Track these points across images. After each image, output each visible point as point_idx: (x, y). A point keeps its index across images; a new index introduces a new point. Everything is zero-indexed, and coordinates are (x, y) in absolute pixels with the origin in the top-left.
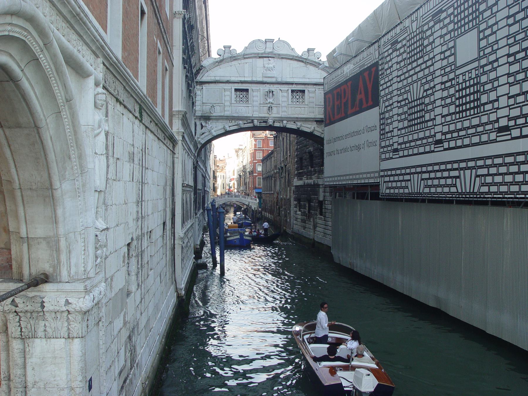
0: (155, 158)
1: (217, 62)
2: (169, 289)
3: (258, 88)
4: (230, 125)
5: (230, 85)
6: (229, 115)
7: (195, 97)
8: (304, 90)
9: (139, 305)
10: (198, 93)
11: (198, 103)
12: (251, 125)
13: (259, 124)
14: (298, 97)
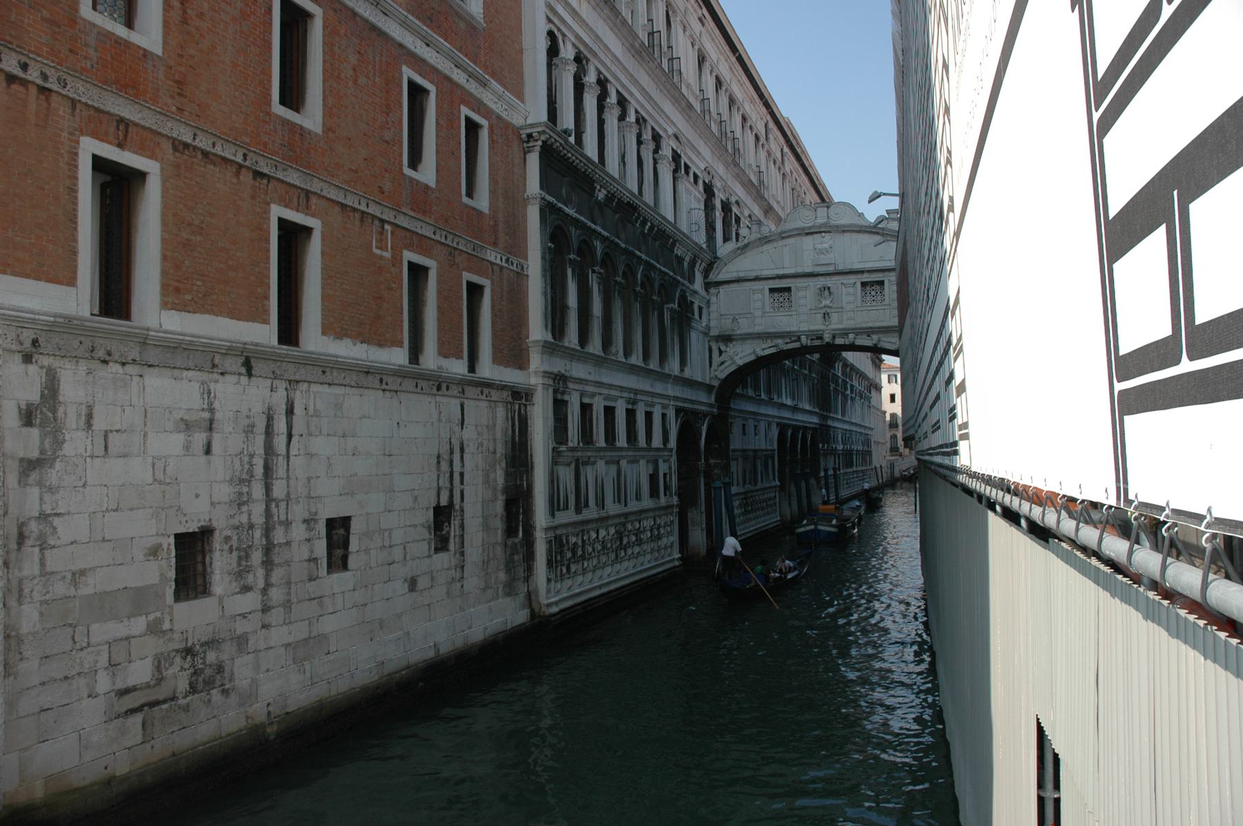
0: (364, 417)
1: (738, 248)
2: (490, 601)
3: (806, 284)
4: (764, 346)
5: (762, 282)
6: (761, 331)
7: (709, 307)
8: (883, 281)
9: (250, 613)
10: (713, 299)
11: (713, 316)
12: (797, 345)
13: (809, 342)
14: (873, 293)
